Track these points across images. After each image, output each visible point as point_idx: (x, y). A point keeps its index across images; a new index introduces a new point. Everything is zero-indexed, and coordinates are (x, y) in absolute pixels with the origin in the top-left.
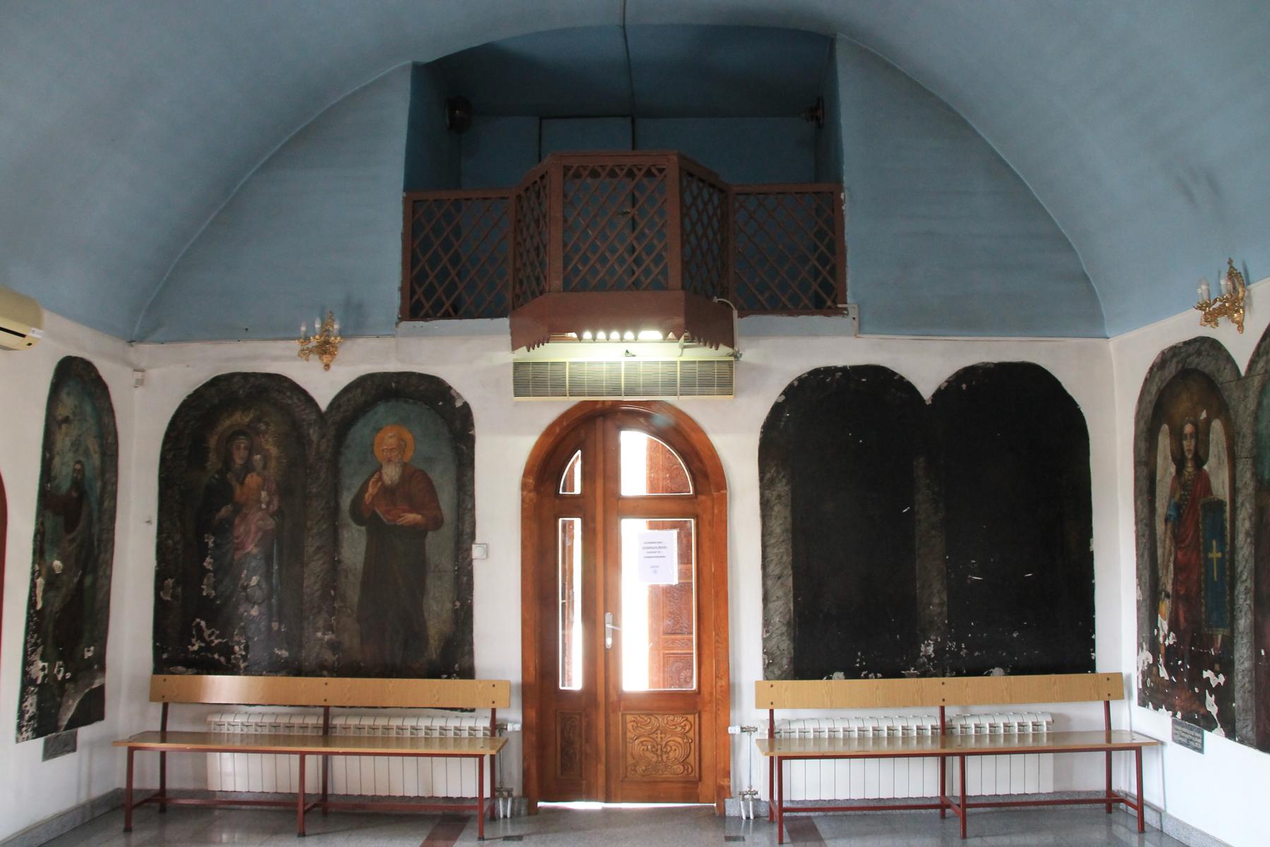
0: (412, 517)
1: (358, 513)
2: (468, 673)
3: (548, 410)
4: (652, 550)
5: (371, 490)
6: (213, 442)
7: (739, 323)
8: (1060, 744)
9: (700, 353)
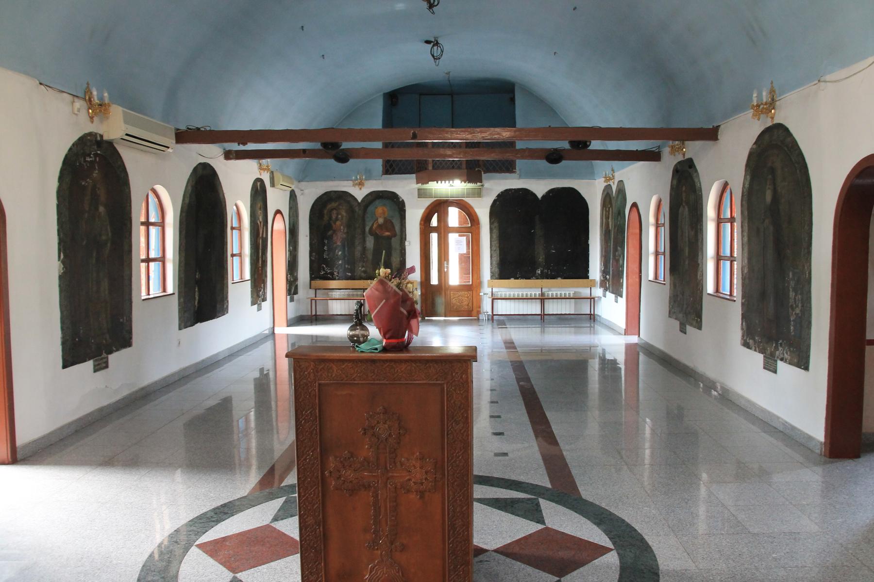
0: (387, 233)
1: (371, 232)
3: (427, 202)
4: (458, 243)
5: (375, 226)
6: (325, 212)
7: (484, 175)
8: (577, 298)
9: (470, 186)
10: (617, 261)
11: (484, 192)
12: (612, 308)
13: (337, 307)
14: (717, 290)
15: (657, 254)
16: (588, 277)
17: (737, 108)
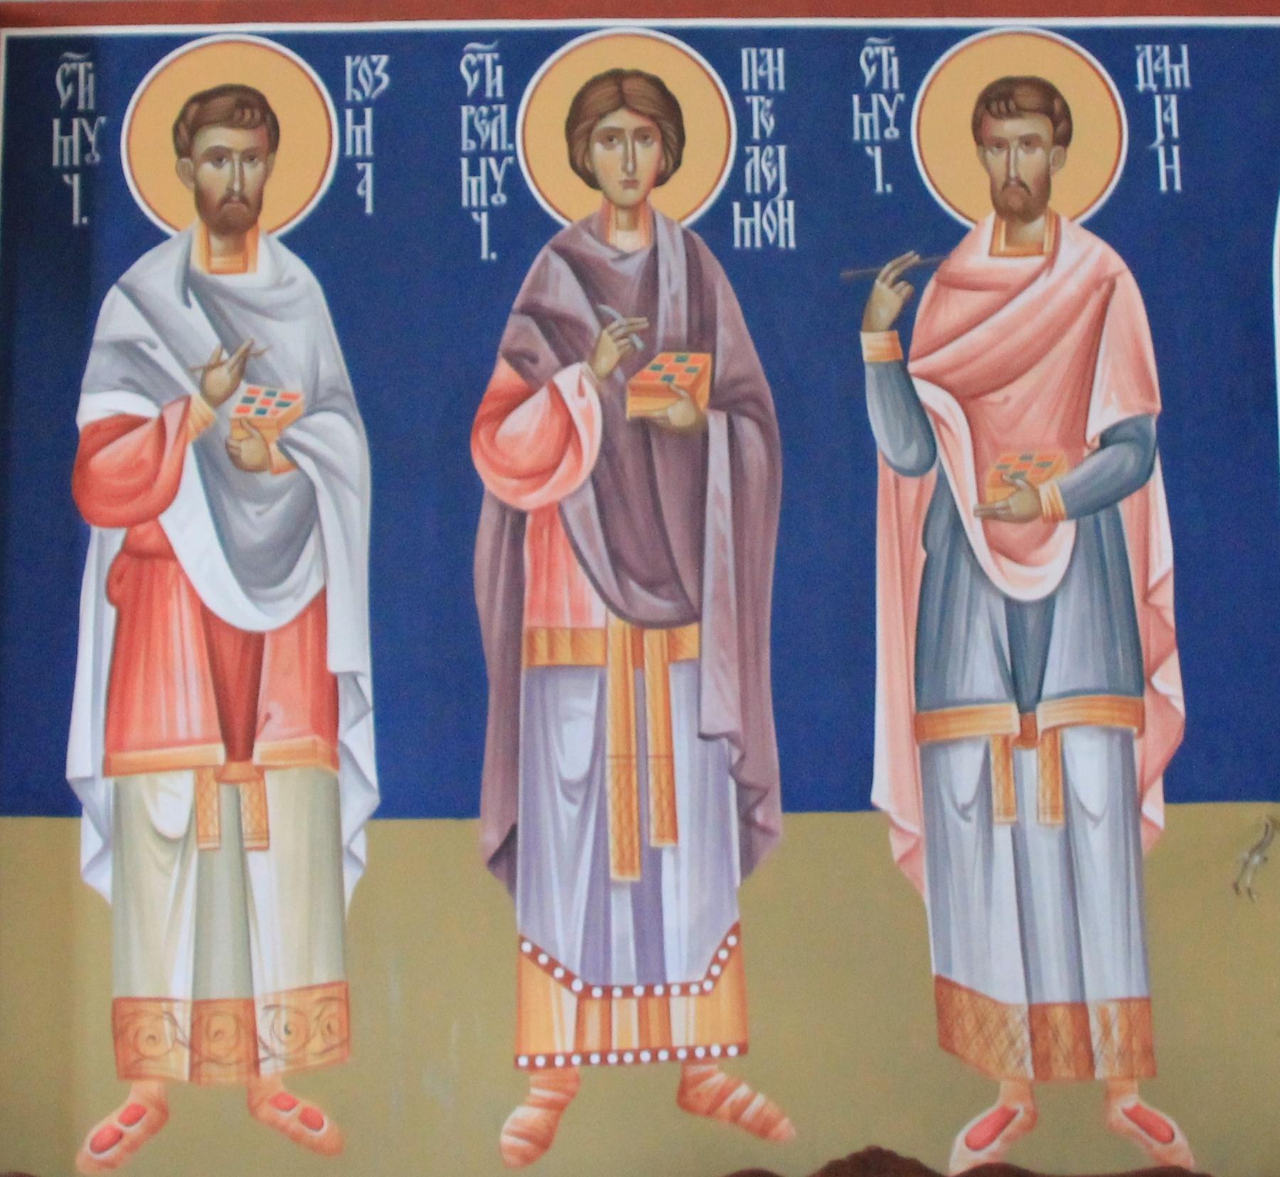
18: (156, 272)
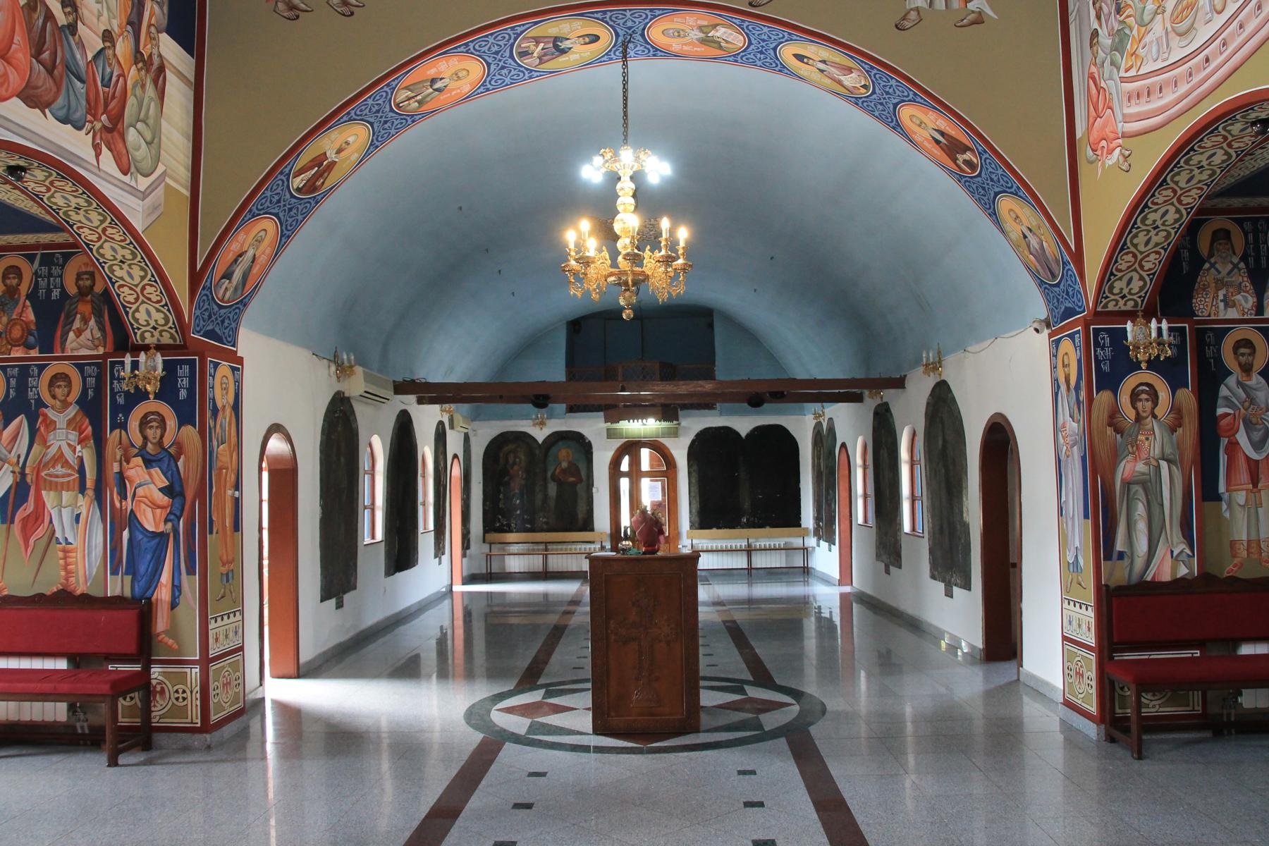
0: (572, 479)
1: (554, 478)
2: (592, 530)
3: (617, 443)
4: (652, 488)
7: (680, 413)
8: (788, 549)
9: (665, 424)
10: (829, 505)
11: (680, 432)
12: (826, 559)
13: (515, 564)
14: (914, 529)
15: (865, 496)
16: (800, 526)
17: (918, 362)
18: (1231, 381)
